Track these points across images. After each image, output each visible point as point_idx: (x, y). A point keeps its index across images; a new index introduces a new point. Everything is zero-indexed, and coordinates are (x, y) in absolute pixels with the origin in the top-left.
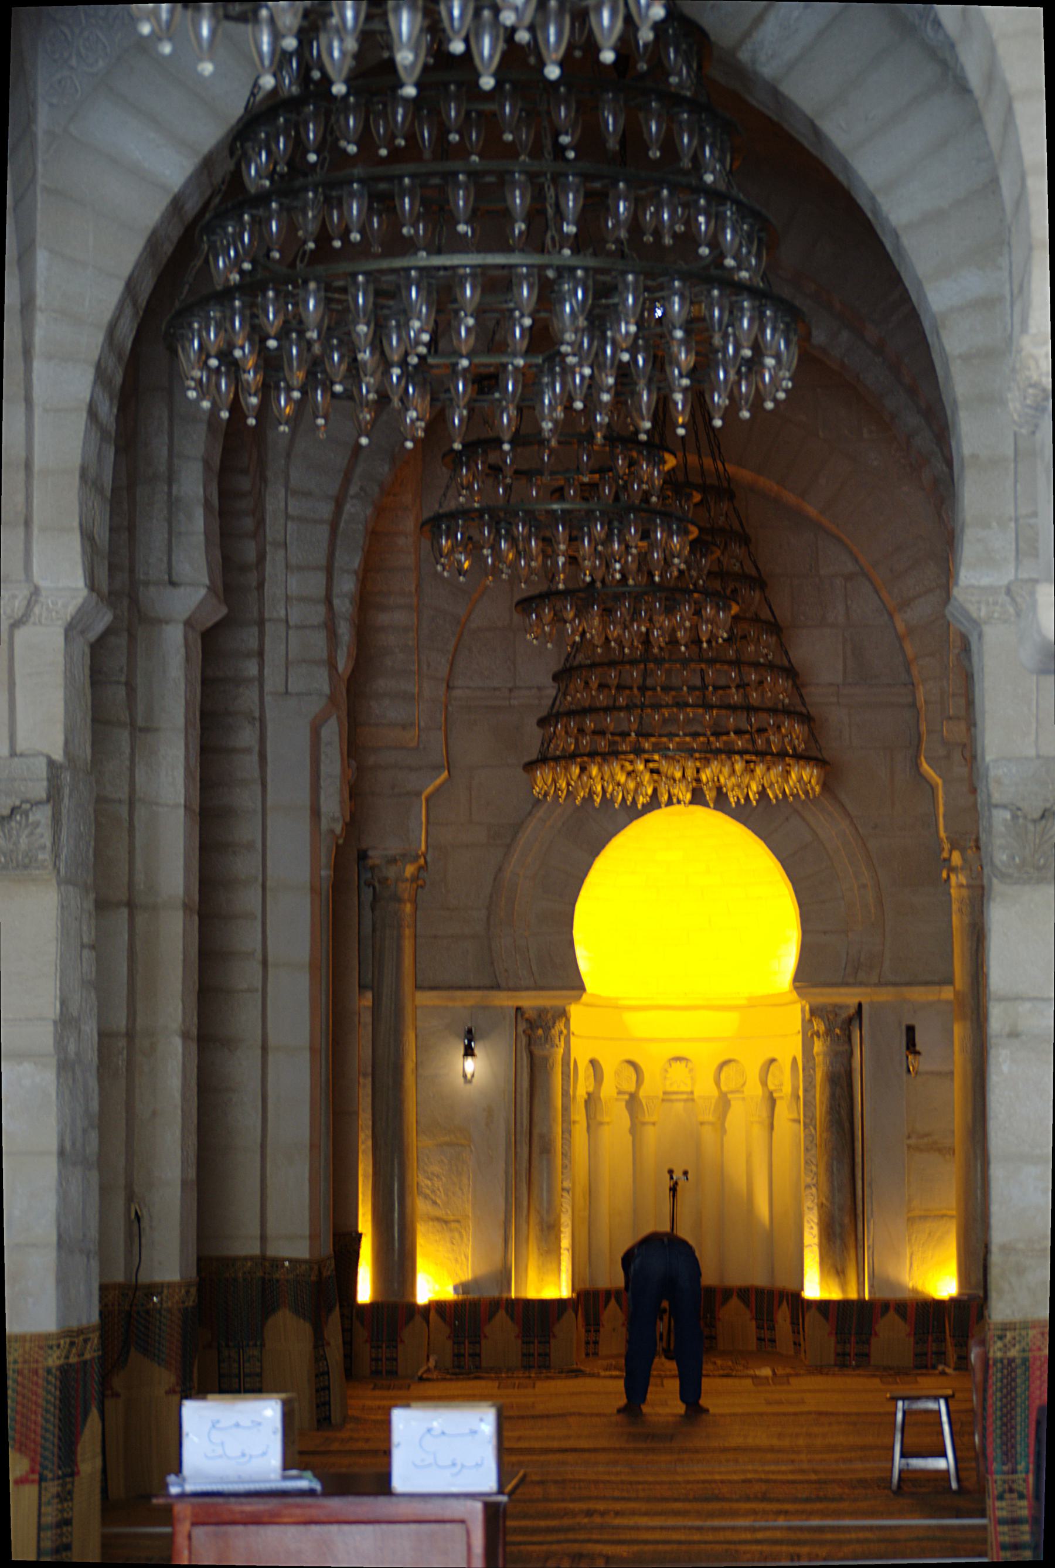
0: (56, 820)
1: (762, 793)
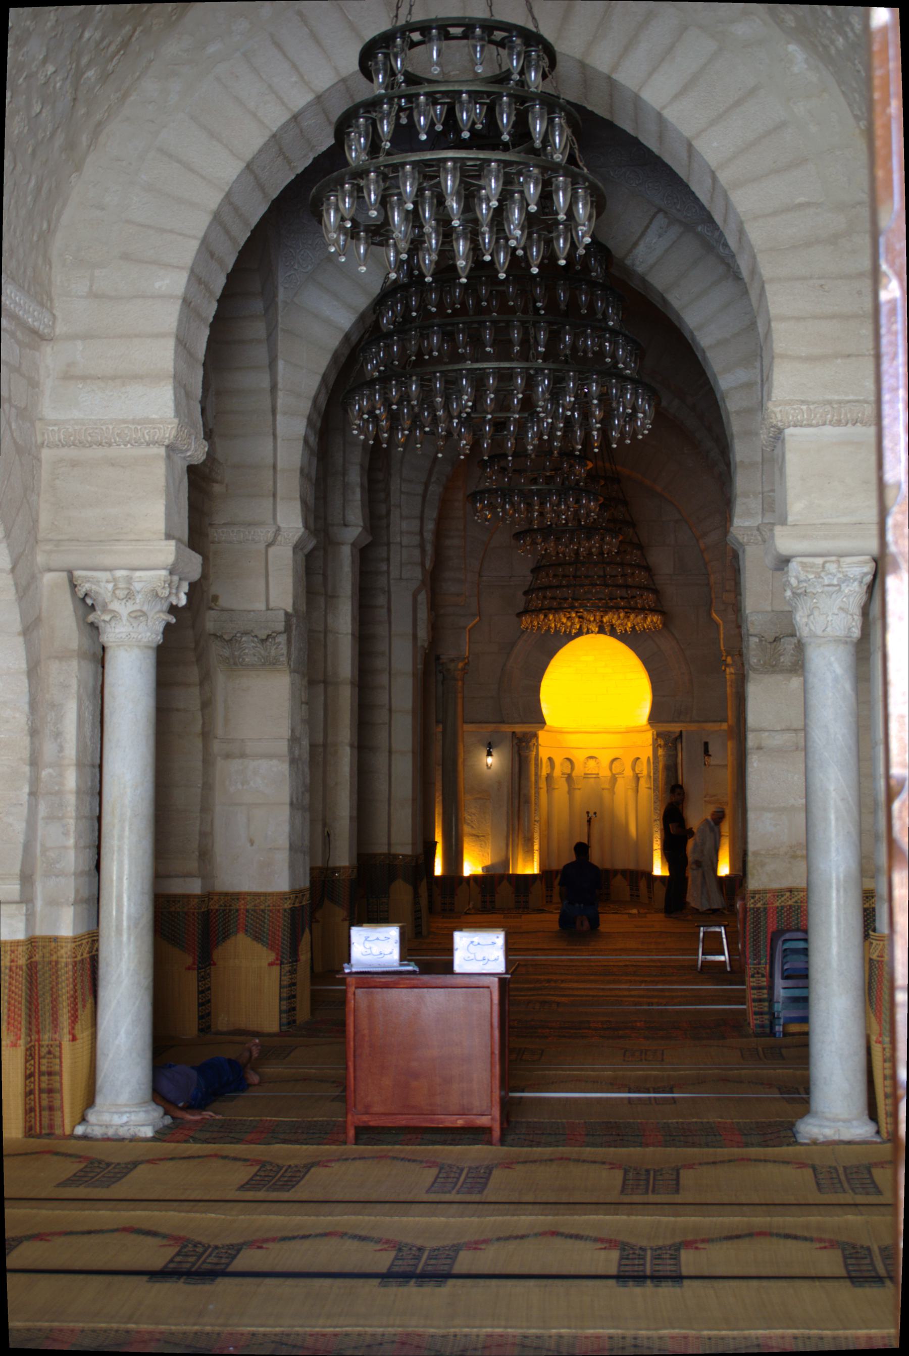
0: (289, 641)
1: (633, 628)
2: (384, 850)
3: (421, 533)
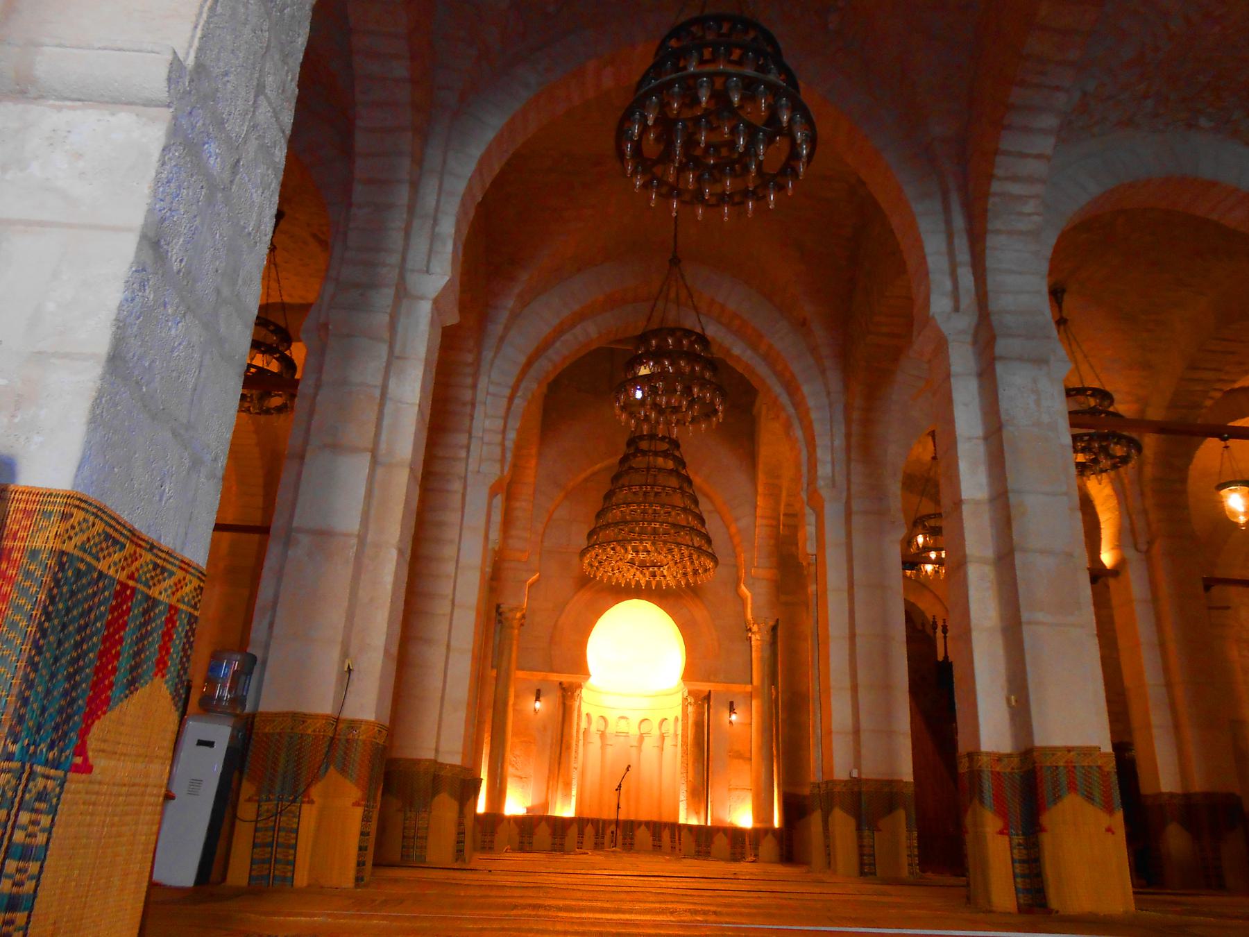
2: (430, 755)
3: (503, 445)
